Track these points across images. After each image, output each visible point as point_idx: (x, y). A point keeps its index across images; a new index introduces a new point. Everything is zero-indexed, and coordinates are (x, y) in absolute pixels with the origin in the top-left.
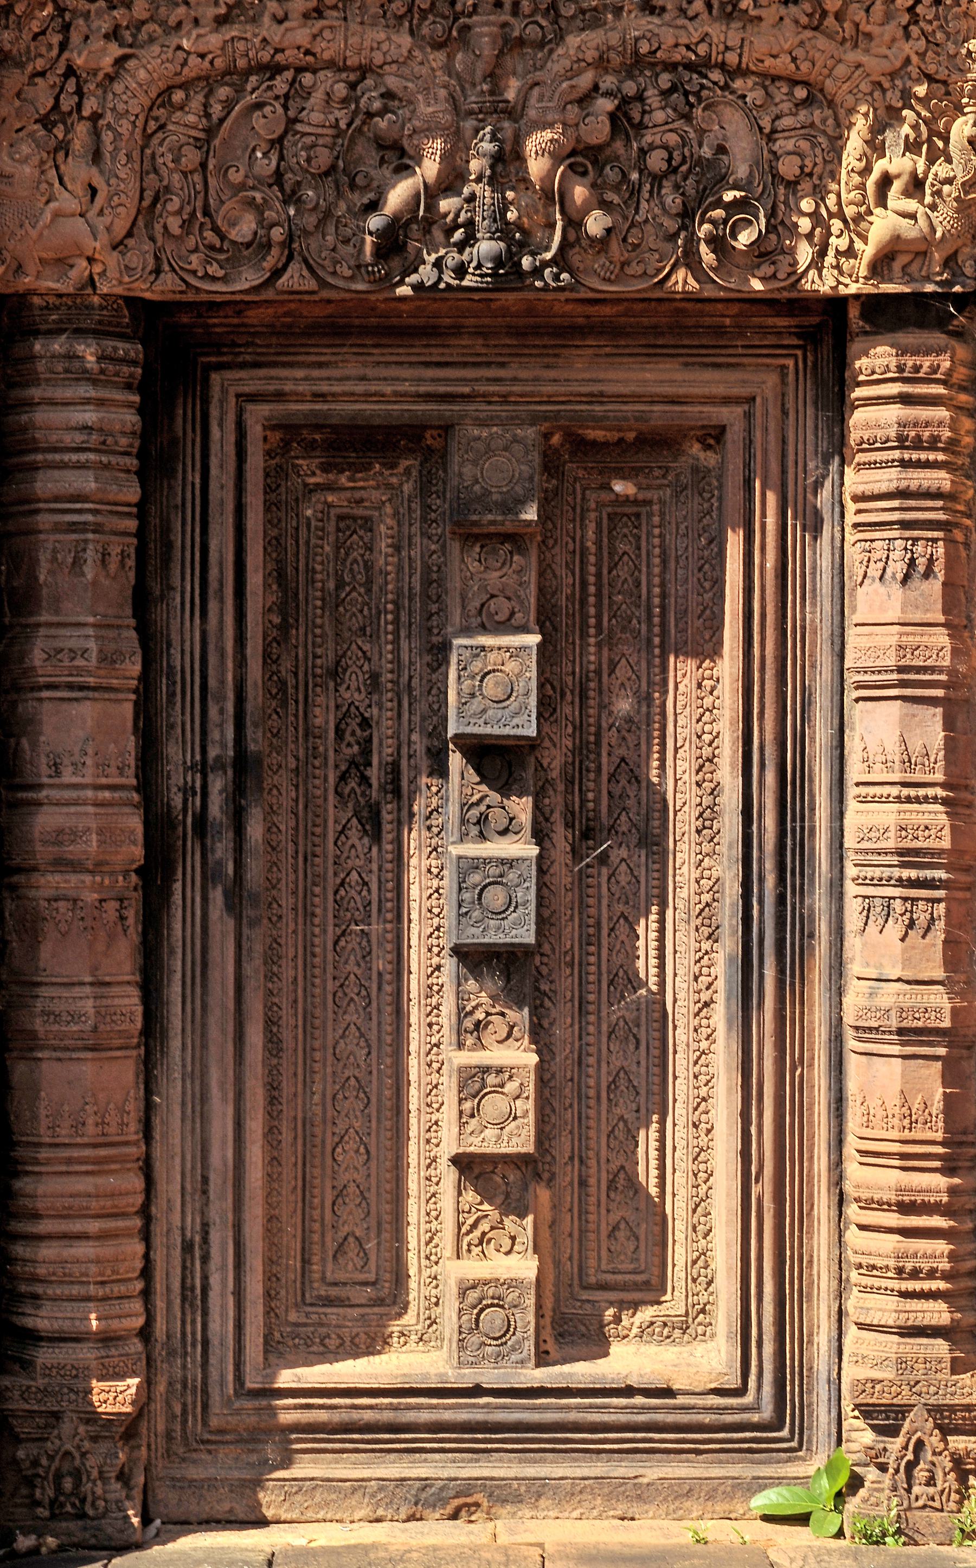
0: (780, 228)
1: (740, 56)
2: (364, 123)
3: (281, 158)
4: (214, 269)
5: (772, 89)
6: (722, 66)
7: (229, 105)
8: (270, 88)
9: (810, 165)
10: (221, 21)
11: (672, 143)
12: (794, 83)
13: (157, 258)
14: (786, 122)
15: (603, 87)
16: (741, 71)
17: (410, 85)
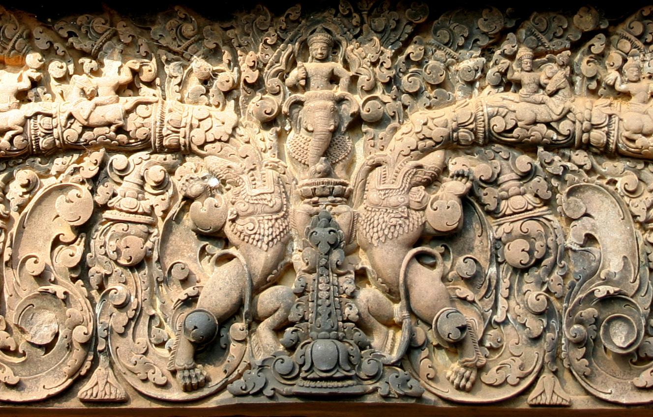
1: (608, 134)
6: (586, 146)
7: (30, 187)
8: (76, 170)
11: (534, 233)
15: (452, 169)
16: (607, 152)
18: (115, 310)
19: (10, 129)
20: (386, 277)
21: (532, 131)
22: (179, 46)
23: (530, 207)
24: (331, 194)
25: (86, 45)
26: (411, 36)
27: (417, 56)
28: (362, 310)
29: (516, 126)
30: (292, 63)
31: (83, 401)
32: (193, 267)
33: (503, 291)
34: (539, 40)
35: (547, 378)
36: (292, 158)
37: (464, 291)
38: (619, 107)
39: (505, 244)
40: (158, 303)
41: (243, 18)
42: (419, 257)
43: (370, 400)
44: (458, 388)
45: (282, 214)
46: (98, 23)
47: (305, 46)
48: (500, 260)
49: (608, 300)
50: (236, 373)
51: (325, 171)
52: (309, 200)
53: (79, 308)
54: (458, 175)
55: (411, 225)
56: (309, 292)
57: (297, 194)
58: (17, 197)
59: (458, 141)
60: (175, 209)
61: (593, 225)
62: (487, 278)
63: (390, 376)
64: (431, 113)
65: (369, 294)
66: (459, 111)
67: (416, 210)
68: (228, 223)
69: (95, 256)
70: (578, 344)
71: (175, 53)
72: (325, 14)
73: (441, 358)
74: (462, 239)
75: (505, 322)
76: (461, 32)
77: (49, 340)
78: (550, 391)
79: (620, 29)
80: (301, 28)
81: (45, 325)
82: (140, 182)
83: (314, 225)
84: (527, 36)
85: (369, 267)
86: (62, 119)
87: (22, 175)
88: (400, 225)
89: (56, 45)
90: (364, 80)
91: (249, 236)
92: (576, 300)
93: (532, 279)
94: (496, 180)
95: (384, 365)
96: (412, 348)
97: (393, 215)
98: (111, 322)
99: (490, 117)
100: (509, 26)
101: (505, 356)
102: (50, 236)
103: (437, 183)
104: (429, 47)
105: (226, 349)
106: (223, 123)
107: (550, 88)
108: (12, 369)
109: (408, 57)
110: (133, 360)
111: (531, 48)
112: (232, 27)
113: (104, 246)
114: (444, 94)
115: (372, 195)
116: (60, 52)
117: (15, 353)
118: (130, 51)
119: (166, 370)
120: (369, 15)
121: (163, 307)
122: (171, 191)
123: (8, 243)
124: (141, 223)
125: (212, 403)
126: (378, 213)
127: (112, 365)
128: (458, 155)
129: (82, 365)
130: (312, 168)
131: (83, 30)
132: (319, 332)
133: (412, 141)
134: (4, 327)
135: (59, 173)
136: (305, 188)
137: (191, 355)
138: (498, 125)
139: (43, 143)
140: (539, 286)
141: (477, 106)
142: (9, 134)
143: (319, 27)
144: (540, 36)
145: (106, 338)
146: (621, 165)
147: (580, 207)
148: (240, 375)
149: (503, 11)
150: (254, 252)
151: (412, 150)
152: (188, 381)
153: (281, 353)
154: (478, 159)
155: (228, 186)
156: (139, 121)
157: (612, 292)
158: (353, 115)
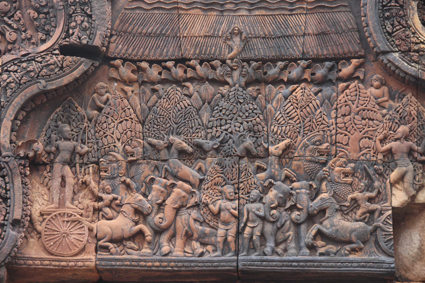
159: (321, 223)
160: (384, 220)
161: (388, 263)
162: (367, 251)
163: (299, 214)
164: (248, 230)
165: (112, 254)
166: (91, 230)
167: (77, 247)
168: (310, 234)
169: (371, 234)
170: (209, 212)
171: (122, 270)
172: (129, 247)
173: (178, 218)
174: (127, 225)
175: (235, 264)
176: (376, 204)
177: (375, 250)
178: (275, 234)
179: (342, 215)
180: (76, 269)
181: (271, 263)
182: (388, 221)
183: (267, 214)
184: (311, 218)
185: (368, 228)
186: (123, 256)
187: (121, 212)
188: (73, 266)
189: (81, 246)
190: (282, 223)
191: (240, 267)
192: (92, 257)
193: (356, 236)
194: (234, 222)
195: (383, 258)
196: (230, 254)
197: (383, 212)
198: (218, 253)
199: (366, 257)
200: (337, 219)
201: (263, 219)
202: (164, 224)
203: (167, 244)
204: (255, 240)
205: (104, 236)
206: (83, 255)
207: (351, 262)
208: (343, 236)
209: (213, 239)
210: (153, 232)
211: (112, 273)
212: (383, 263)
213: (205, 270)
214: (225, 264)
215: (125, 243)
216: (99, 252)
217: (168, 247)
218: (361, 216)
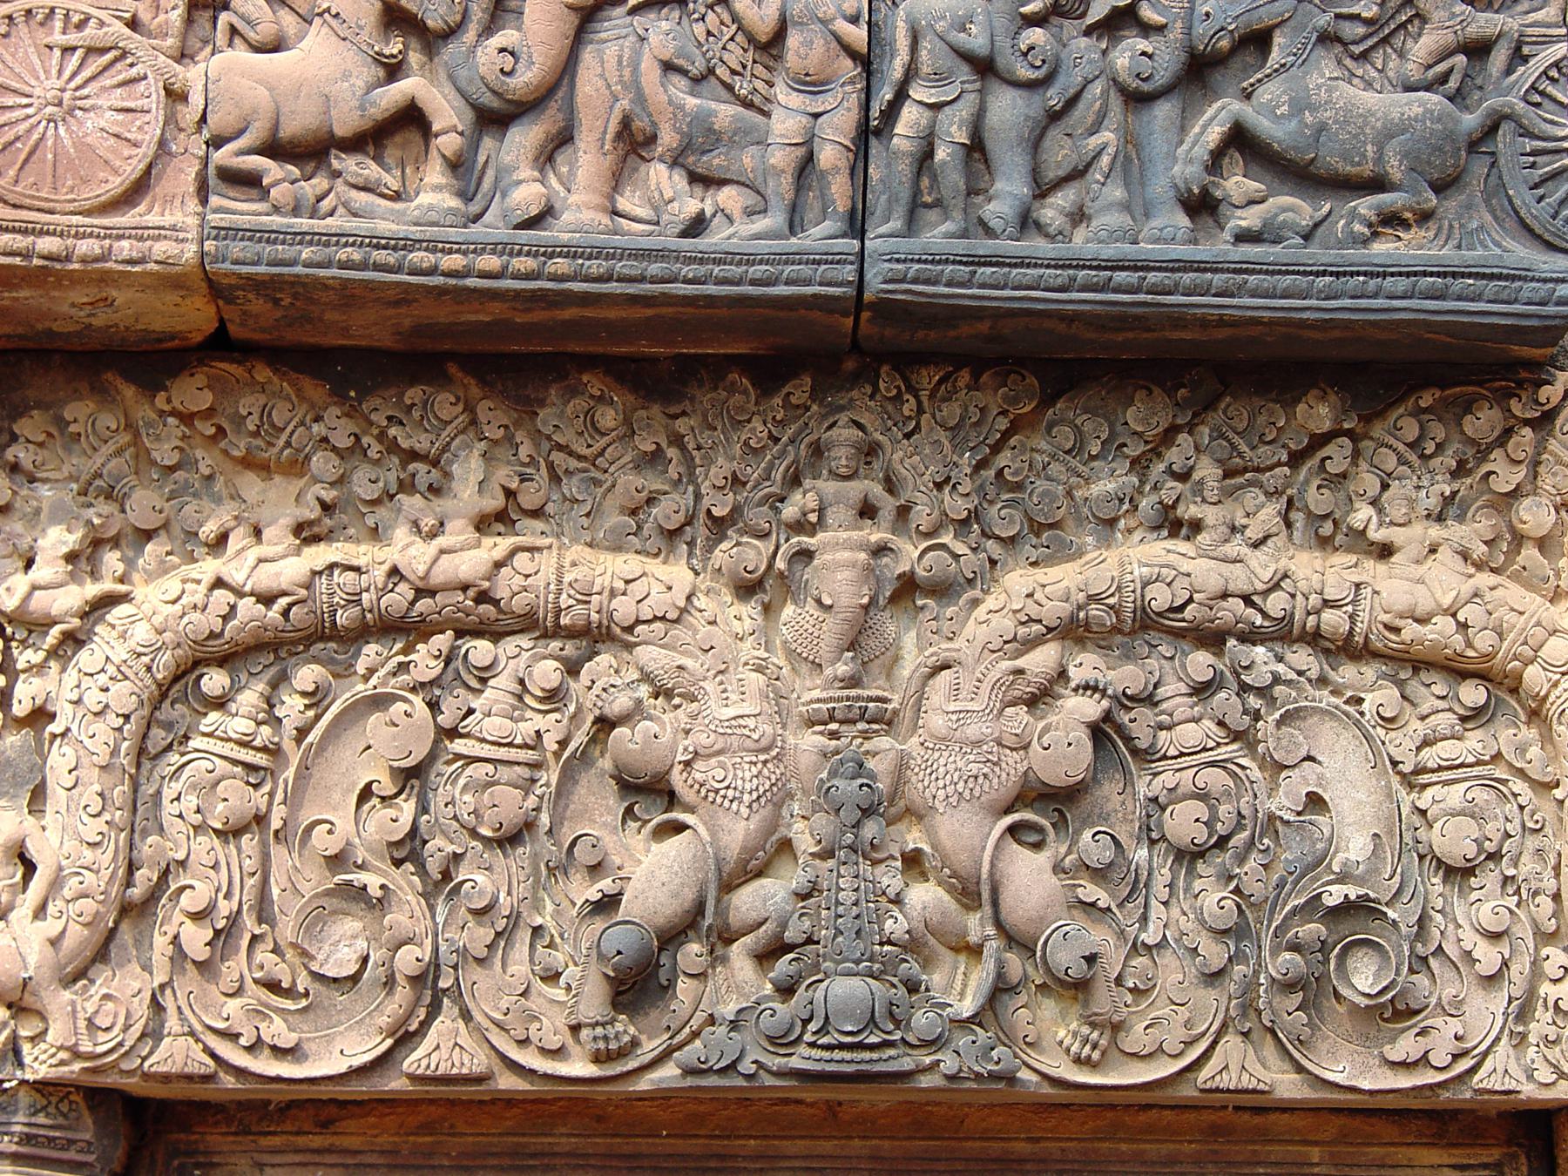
0: (1433, 962)
1: (1352, 617)
2: (593, 740)
3: (423, 808)
4: (278, 1031)
5: (1414, 687)
6: (1314, 639)
7: (317, 698)
8: (403, 667)
9: (1497, 837)
10: (306, 534)
11: (1216, 789)
12: (1457, 670)
13: (157, 1006)
14: (1446, 750)
15: (1076, 675)
16: (1350, 649)
17: (688, 662)
18: (470, 917)
19: (285, 594)
20: (957, 866)
21: (1219, 610)
22: (589, 446)
23: (1211, 744)
24: (862, 718)
25: (421, 442)
26: (1007, 435)
27: (1015, 474)
28: (915, 924)
29: (1190, 600)
30: (794, 481)
31: (413, 1078)
32: (609, 841)
33: (1160, 890)
34: (1233, 446)
35: (1231, 1041)
36: (791, 654)
37: (1092, 892)
38: (1371, 569)
39: (1163, 809)
40: (549, 907)
41: (706, 398)
42: (1012, 830)
43: (925, 1081)
44: (1078, 1060)
45: (774, 753)
46: (445, 404)
47: (818, 450)
48: (1154, 835)
49: (1348, 908)
50: (687, 1030)
51: (852, 678)
52: (822, 728)
53: (408, 912)
54: (1086, 687)
55: (1004, 775)
56: (821, 892)
57: (801, 715)
58: (294, 714)
59: (1087, 625)
60: (579, 739)
61: (1321, 777)
62: (1133, 867)
63: (963, 1041)
64: (1040, 575)
65: (926, 897)
66: (1091, 573)
67: (1012, 749)
68: (678, 768)
69: (437, 820)
70: (1289, 986)
71: (580, 458)
72: (855, 394)
73: (1049, 1008)
74: (1089, 798)
75: (1162, 944)
76: (1096, 431)
77: (352, 969)
78: (1242, 1067)
79: (1378, 430)
80: (810, 418)
81: (343, 945)
82: (517, 688)
83: (833, 774)
84: (1212, 439)
85: (927, 848)
86: (379, 574)
87: (307, 675)
88: (985, 775)
89: (365, 440)
90: (922, 515)
91: (717, 791)
92: (1287, 908)
93: (1211, 871)
94: (1151, 695)
95: (951, 1021)
96: (1001, 989)
97: (972, 758)
98: (462, 939)
99: (1145, 585)
100: (1179, 421)
101: (1158, 1003)
102: (354, 784)
103: (1048, 700)
104: (1038, 457)
105: (668, 988)
106: (670, 588)
107: (1253, 533)
108: (285, 1021)
109: (1000, 473)
110: (504, 1005)
111: (1219, 461)
112: (684, 413)
113: (452, 802)
114: (1063, 541)
115: (936, 722)
116: (373, 453)
117: (289, 993)
118: (500, 452)
119: (561, 1021)
120: (932, 396)
121: (557, 913)
122: (572, 708)
123: (279, 797)
124: (519, 764)
125: (644, 1084)
126: (946, 754)
127: (466, 1015)
128: (1084, 649)
129: (410, 1015)
130: (828, 671)
131: (416, 414)
132: (838, 963)
133: (1007, 625)
134: (271, 946)
135: (371, 671)
136: (815, 706)
137: (609, 1000)
138: (1160, 598)
139: (342, 618)
140: (1223, 881)
141: (1122, 564)
142: (283, 602)
143: (843, 418)
144: (1236, 439)
145: (455, 967)
146: (1370, 671)
147: (1298, 745)
148: (696, 1034)
149: (1170, 392)
150: (725, 820)
151: (1006, 642)
152: (602, 1045)
153: (768, 998)
154: (1119, 657)
155: (677, 701)
156: (518, 581)
157: (1353, 897)
158: (900, 576)
159: (1248, 96)
160: (1533, 87)
161: (1545, 281)
162: (1451, 226)
163: (1150, 50)
164: (910, 119)
165: (276, 209)
166: (175, 96)
167: (116, 172)
168: (1194, 144)
169: (1473, 146)
170: (734, 27)
171: (322, 284)
172: (360, 181)
173: (588, 56)
174: (346, 76)
175: (849, 272)
176: (1497, 12)
177: (1488, 218)
178: (1035, 144)
179: (1339, 62)
180: (109, 271)
181: (1015, 271)
182: (1549, 89)
183: (1003, 43)
184: (1200, 71)
185: (1457, 122)
186: (329, 220)
187: (320, 15)
188: (96, 260)
189: (132, 169)
190: (1072, 91)
191: (875, 284)
192: (185, 215)
193: (1405, 155)
194: (852, 82)
195: (1521, 253)
196: (828, 226)
197: (1526, 50)
198: (774, 220)
199: (1446, 253)
200: (1323, 76)
201: (984, 67)
202: (526, 78)
203: (536, 174)
204: (944, 163)
205: (242, 126)
206: (141, 208)
207: (1378, 275)
208: (1346, 157)
209: (748, 159)
210: (469, 115)
211: (276, 302)
212: (1520, 278)
213: (711, 300)
214: (805, 270)
215: (335, 164)
216: (214, 200)
217: (538, 188)
218: (1430, 67)
